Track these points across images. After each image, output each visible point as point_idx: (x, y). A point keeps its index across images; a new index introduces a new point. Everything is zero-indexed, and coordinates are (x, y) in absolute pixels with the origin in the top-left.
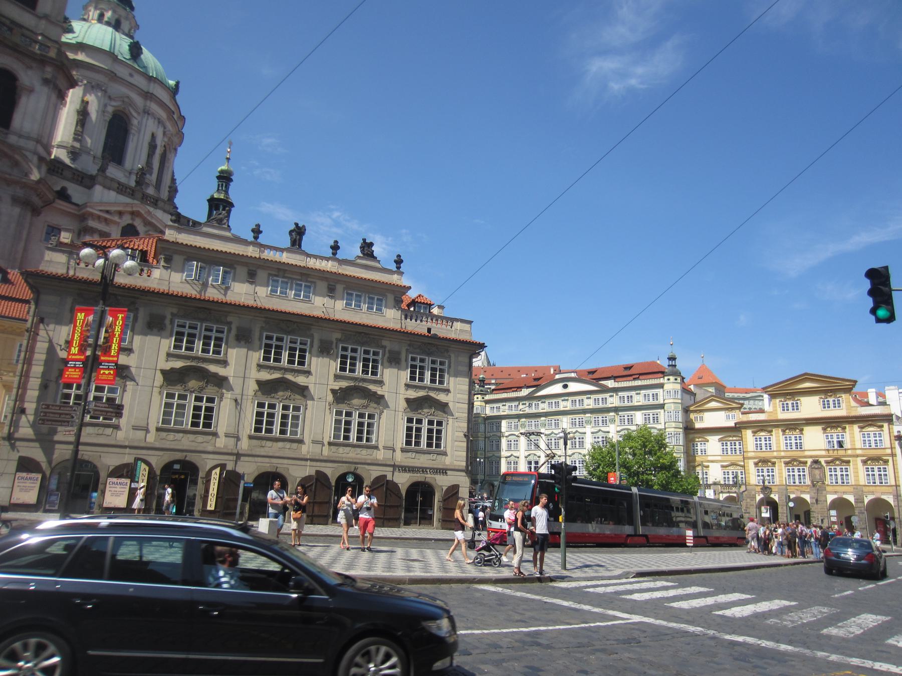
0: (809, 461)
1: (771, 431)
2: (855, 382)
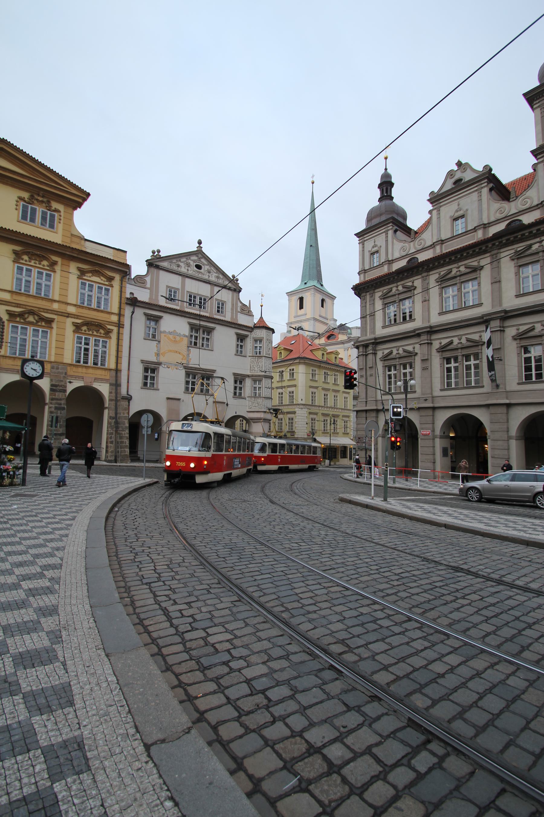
2: (88, 195)
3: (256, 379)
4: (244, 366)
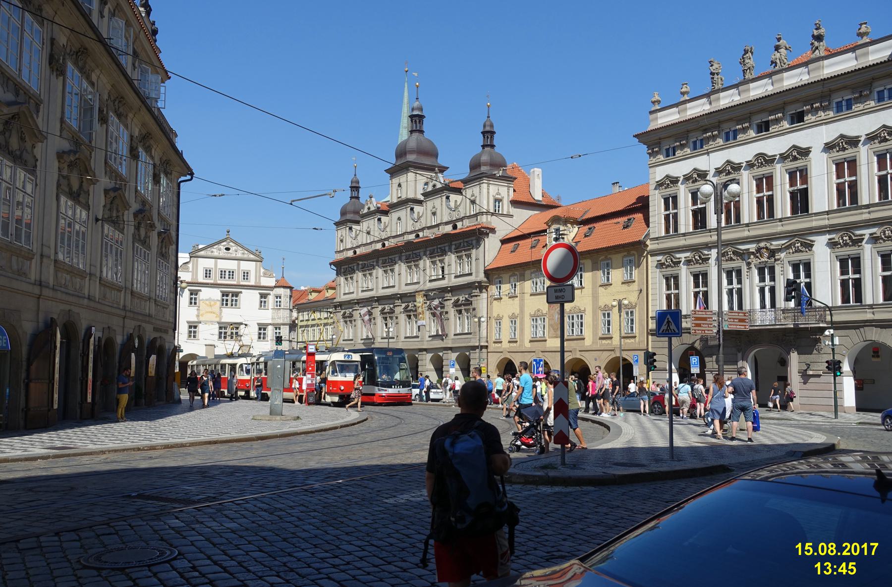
3: (277, 327)
4: (266, 316)
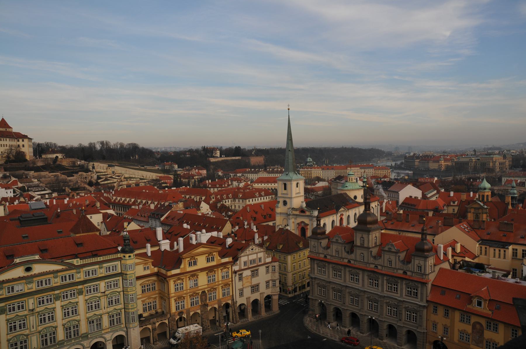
0: (201, 291)
1: (182, 280)
3: (274, 281)
4: (269, 277)
